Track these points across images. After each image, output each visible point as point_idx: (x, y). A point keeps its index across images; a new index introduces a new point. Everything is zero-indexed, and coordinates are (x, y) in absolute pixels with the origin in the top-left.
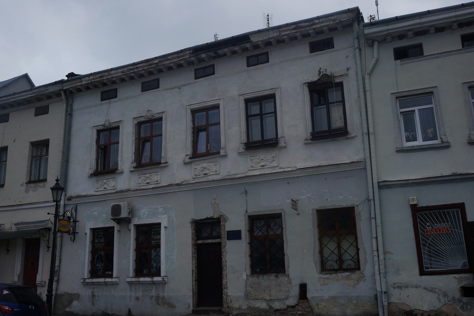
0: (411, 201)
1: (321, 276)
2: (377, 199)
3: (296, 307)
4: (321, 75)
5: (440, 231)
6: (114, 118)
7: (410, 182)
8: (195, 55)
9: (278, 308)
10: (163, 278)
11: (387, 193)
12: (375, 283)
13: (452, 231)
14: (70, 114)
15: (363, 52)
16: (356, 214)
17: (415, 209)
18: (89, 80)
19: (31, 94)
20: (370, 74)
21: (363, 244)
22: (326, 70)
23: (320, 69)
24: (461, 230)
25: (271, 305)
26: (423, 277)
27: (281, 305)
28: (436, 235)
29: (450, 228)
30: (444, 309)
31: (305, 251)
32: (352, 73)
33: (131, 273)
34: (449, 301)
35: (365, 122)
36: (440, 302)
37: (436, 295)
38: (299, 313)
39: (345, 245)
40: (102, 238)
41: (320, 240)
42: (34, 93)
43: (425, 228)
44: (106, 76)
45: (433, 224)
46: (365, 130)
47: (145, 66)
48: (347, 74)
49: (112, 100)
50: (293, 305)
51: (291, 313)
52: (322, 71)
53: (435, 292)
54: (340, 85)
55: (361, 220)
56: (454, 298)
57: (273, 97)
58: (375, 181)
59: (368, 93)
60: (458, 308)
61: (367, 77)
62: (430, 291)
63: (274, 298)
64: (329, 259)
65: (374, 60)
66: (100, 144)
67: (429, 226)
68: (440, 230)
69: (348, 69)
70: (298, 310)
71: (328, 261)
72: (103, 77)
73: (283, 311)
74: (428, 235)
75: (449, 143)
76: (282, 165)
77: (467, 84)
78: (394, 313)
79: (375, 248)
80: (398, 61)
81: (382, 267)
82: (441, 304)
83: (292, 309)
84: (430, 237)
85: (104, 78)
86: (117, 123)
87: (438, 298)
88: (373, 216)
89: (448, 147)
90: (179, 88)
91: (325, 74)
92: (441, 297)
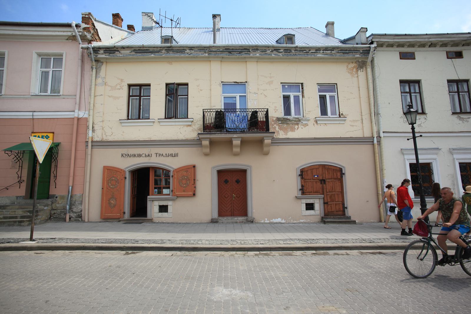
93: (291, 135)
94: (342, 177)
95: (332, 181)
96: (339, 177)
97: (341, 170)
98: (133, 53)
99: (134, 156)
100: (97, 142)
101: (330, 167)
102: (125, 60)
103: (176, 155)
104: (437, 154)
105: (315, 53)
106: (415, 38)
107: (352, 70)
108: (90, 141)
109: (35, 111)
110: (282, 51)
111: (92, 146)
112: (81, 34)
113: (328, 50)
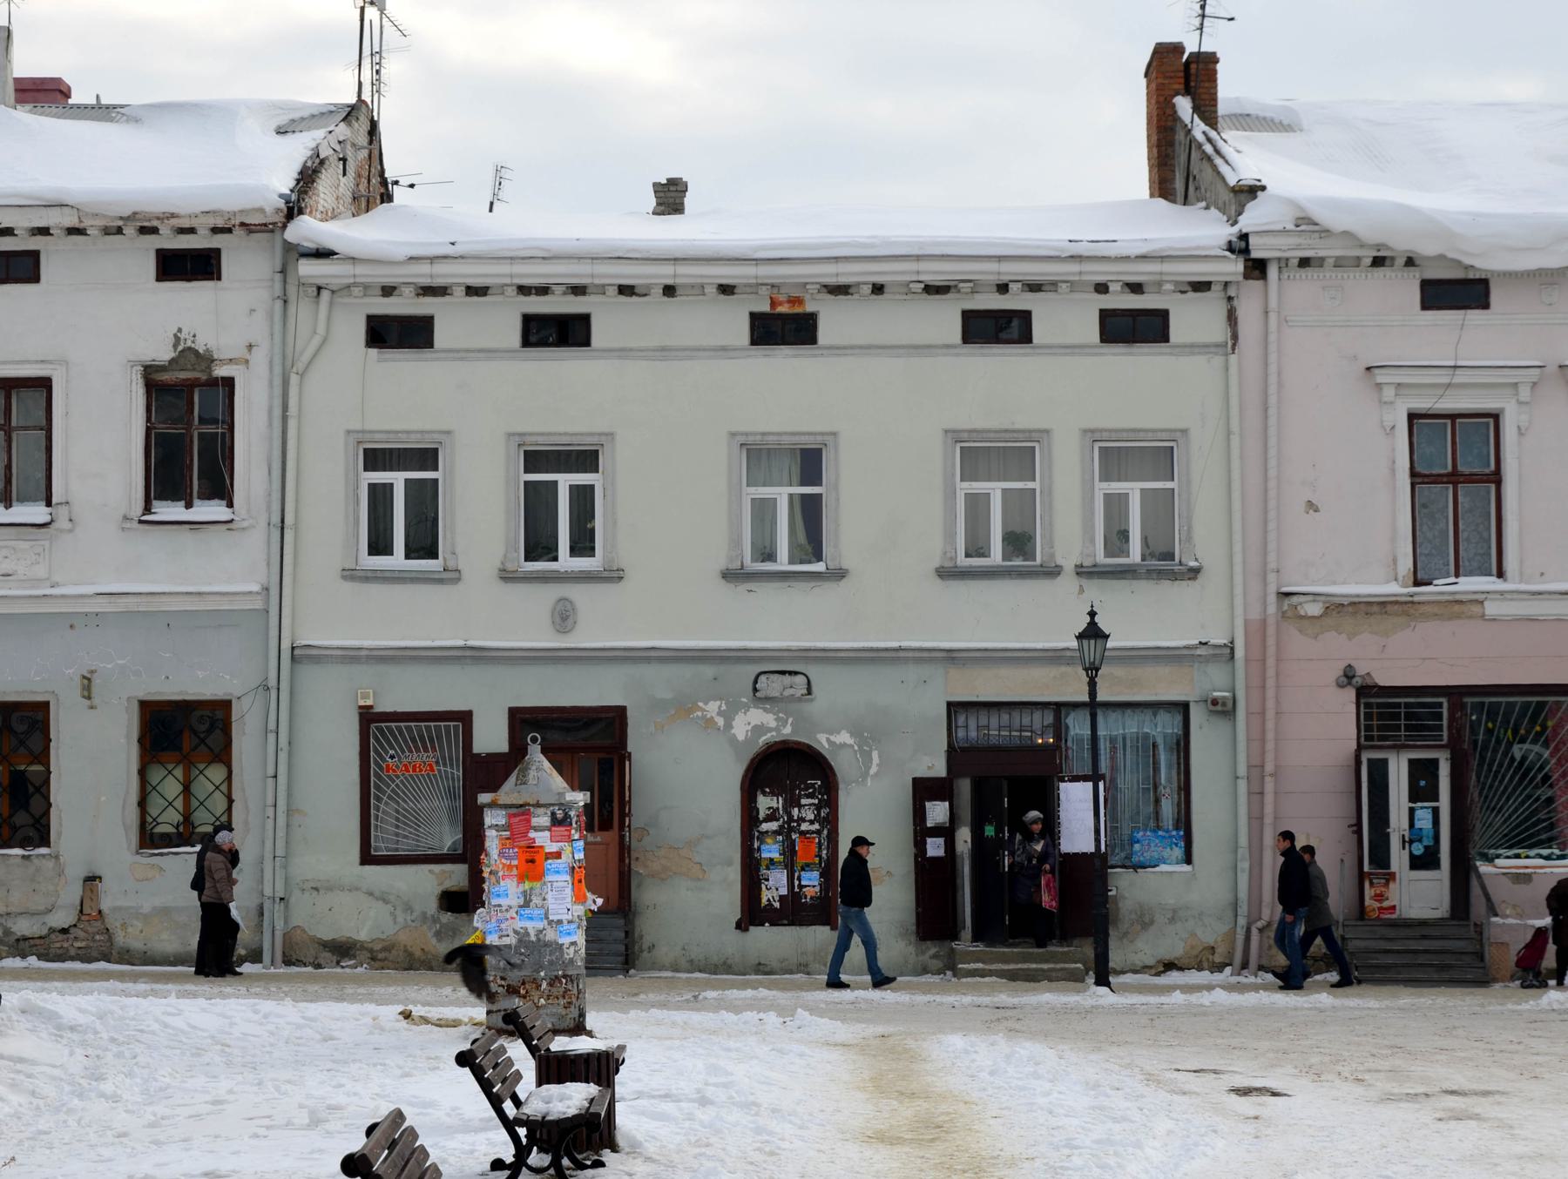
0: (362, 698)
1: (138, 857)
2: (284, 686)
3: (72, 930)
4: (180, 348)
5: (414, 771)
7: (364, 653)
9: (28, 933)
11: (308, 672)
12: (262, 882)
13: (439, 771)
15: (292, 309)
16: (233, 719)
17: (368, 718)
20: (302, 375)
21: (243, 790)
22: (194, 336)
23: (180, 330)
24: (458, 771)
25: (8, 926)
26: (367, 868)
27: (35, 927)
28: (406, 778)
29: (437, 763)
30: (403, 938)
31: (103, 799)
32: (259, 358)
34: (413, 921)
35: (276, 496)
36: (395, 923)
37: (389, 906)
38: (78, 944)
39: (202, 787)
41: (142, 773)
43: (383, 760)
45: (403, 752)
46: (276, 519)
48: (247, 362)
50: (66, 926)
51: (58, 945)
52: (182, 336)
53: (386, 902)
54: (229, 383)
55: (244, 734)
56: (424, 915)
57: (45, 384)
58: (286, 645)
59: (292, 424)
60: (430, 935)
61: (294, 379)
62: (377, 899)
63: (19, 911)
64: (159, 820)
65: (316, 341)
67: (392, 757)
68: (414, 767)
69: (250, 346)
70: (76, 938)
71: (158, 824)
73: (38, 942)
74: (389, 777)
75: (457, 573)
76: (56, 578)
77: (517, 438)
78: (297, 944)
79: (270, 801)
80: (374, 352)
81: (280, 844)
82: (397, 928)
83: (61, 937)
84: (393, 781)
87: (392, 914)
88: (272, 725)
89: (458, 580)
91: (190, 349)
92: (399, 912)
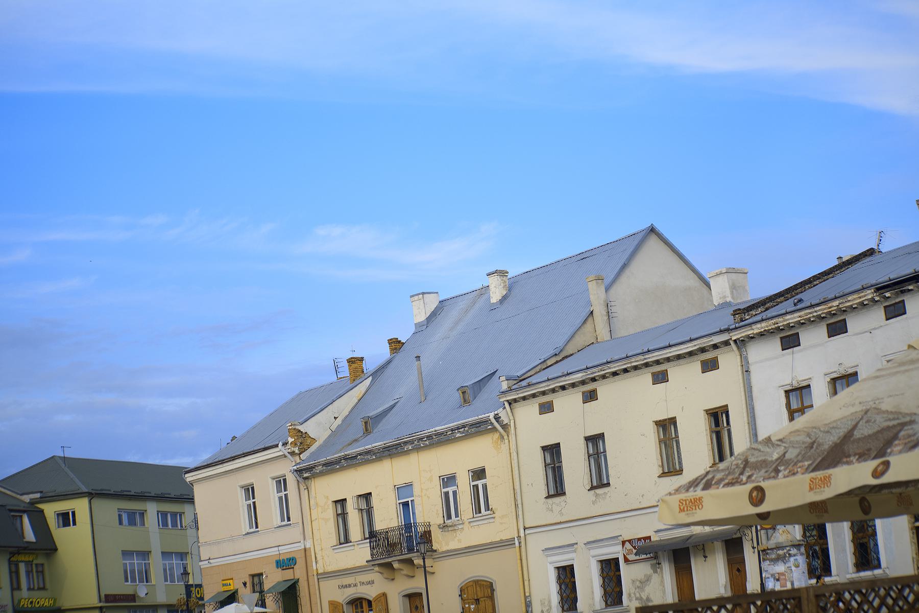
6: (800, 376)
8: (878, 294)
10: (884, 571)
14: (747, 371)
18: (762, 328)
19: (692, 347)
33: (851, 567)
40: (813, 530)
42: (695, 346)
44: (780, 322)
47: (825, 309)
49: (795, 349)
66: (792, 408)
72: (777, 323)
85: (779, 325)
86: (807, 381)
90: (871, 333)
93: (453, 545)
94: (492, 594)
95: (485, 600)
96: (490, 595)
97: (491, 584)
98: (324, 468)
99: (346, 586)
100: (321, 574)
101: (482, 583)
102: (322, 474)
103: (373, 582)
104: (575, 551)
105: (452, 434)
106: (536, 389)
107: (497, 442)
108: (315, 574)
109: (279, 546)
110: (426, 439)
111: (318, 579)
112: (289, 451)
113: (461, 428)
